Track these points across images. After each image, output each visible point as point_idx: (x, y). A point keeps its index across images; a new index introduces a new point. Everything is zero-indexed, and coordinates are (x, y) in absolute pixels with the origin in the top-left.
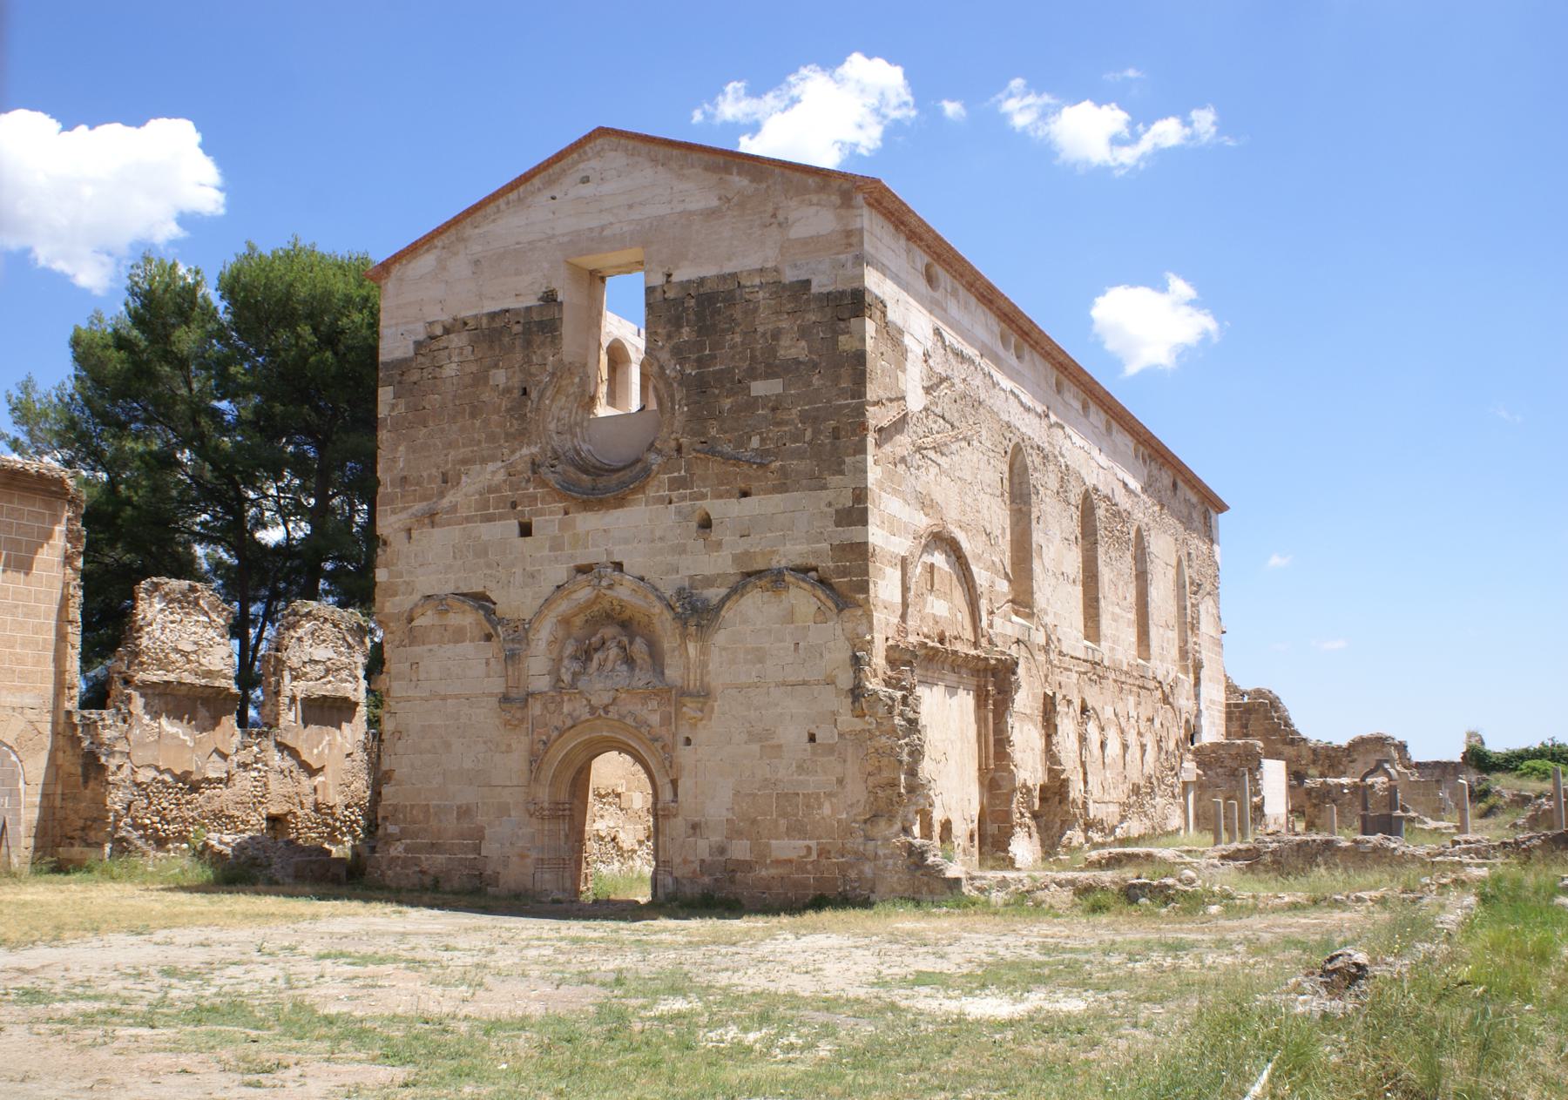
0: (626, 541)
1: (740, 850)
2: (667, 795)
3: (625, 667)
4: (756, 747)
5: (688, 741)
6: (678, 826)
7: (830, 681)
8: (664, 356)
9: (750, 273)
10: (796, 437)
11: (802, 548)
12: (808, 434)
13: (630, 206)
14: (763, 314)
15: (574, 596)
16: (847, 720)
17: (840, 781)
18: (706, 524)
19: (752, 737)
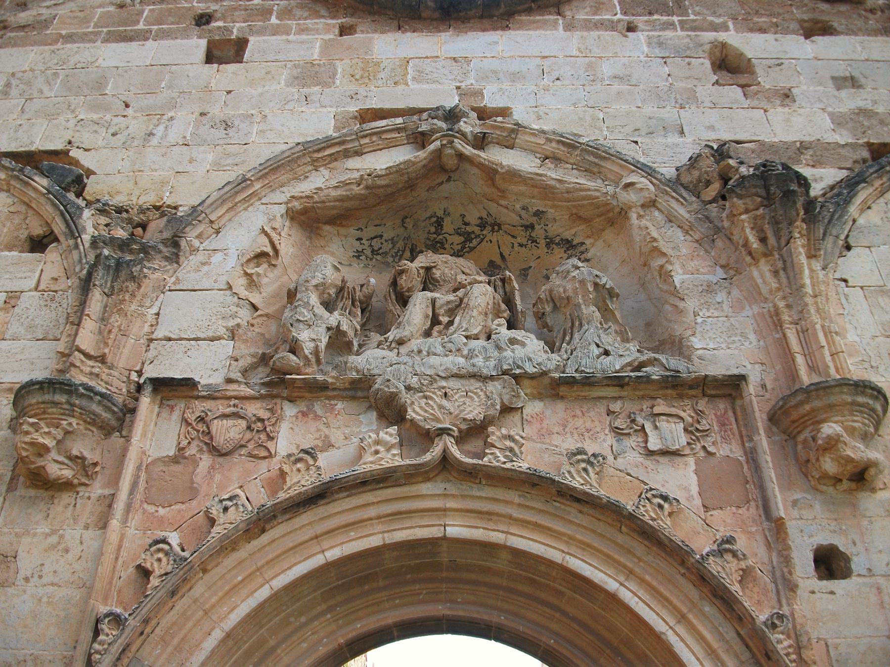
0: (515, 77)
15: (354, 163)
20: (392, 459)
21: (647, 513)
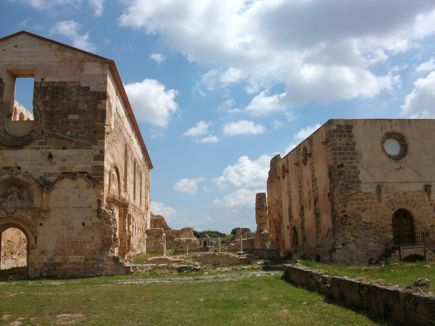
0: (22, 160)
1: (58, 259)
2: (33, 242)
3: (19, 200)
4: (64, 227)
5: (41, 225)
6: (37, 251)
7: (90, 206)
8: (39, 104)
9: (70, 82)
10: (83, 133)
11: (83, 166)
12: (86, 132)
13: (31, 57)
14: (74, 95)
15: (2, 177)
16: (96, 219)
17: (93, 238)
18: (50, 156)
19: (63, 224)
20: (6, 216)
21: (26, 221)
